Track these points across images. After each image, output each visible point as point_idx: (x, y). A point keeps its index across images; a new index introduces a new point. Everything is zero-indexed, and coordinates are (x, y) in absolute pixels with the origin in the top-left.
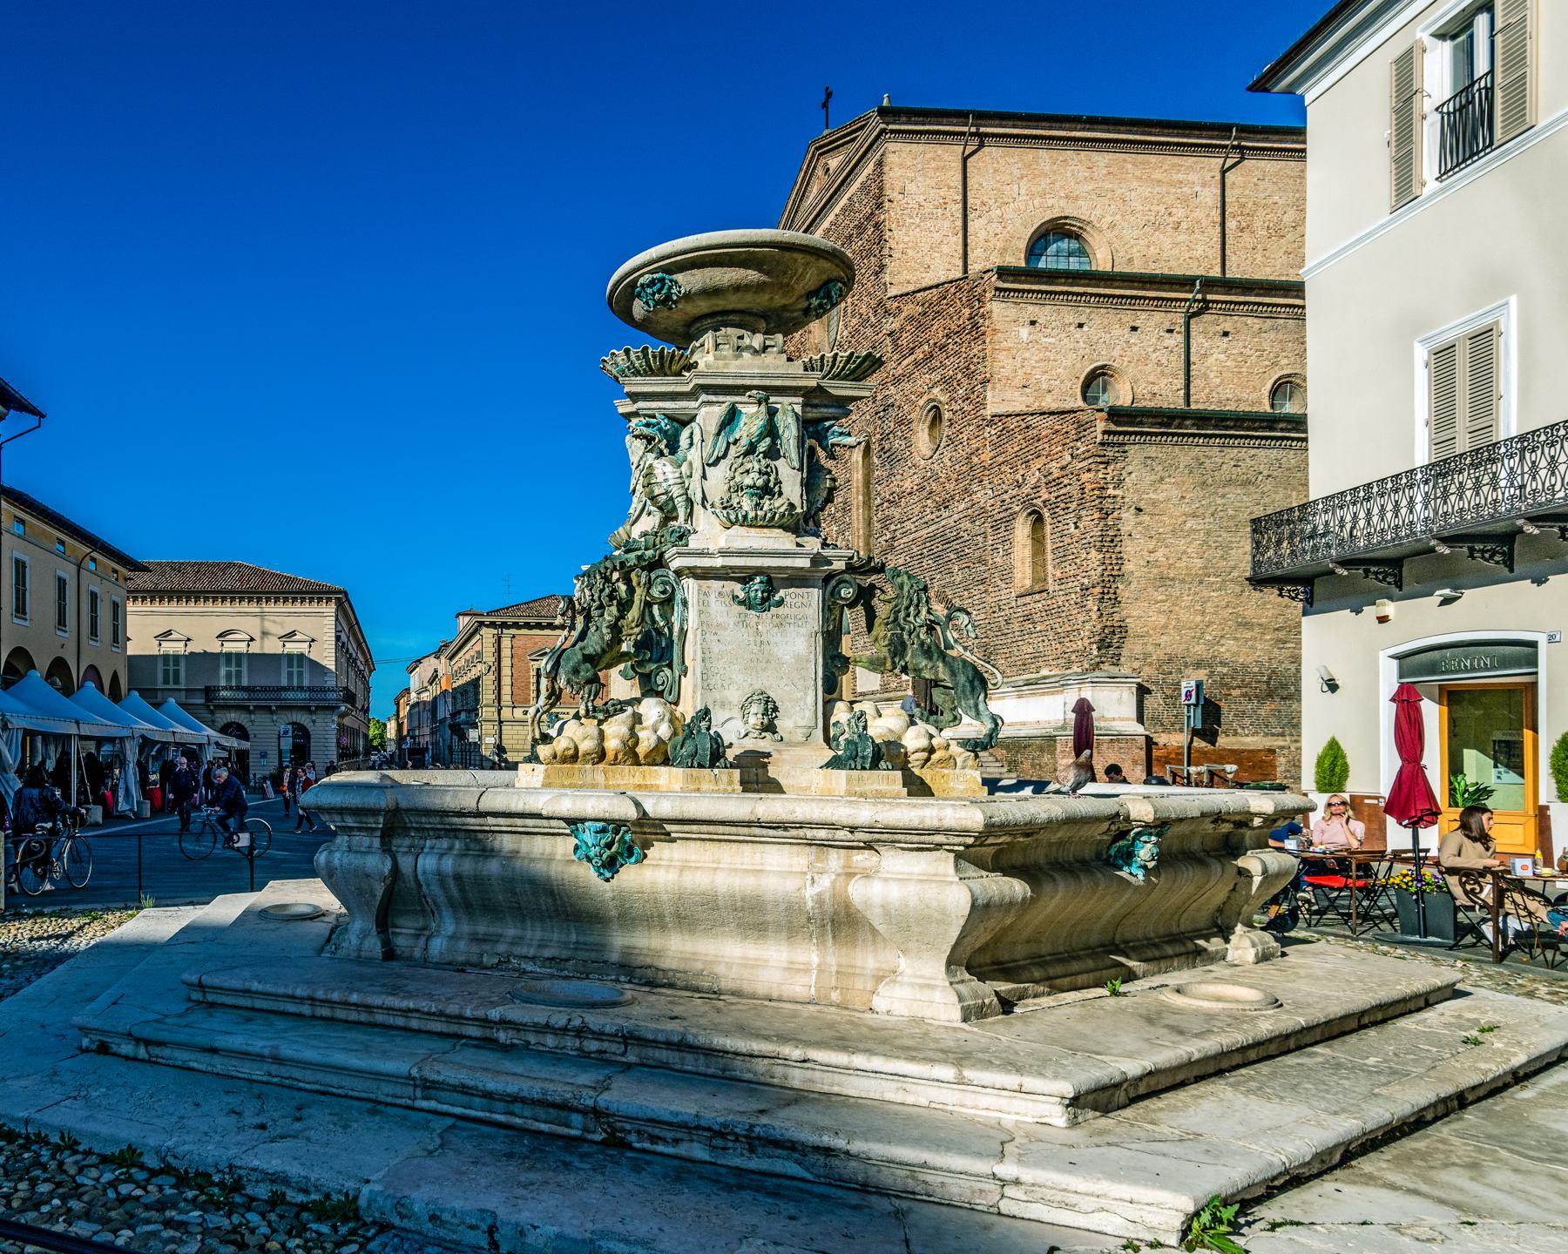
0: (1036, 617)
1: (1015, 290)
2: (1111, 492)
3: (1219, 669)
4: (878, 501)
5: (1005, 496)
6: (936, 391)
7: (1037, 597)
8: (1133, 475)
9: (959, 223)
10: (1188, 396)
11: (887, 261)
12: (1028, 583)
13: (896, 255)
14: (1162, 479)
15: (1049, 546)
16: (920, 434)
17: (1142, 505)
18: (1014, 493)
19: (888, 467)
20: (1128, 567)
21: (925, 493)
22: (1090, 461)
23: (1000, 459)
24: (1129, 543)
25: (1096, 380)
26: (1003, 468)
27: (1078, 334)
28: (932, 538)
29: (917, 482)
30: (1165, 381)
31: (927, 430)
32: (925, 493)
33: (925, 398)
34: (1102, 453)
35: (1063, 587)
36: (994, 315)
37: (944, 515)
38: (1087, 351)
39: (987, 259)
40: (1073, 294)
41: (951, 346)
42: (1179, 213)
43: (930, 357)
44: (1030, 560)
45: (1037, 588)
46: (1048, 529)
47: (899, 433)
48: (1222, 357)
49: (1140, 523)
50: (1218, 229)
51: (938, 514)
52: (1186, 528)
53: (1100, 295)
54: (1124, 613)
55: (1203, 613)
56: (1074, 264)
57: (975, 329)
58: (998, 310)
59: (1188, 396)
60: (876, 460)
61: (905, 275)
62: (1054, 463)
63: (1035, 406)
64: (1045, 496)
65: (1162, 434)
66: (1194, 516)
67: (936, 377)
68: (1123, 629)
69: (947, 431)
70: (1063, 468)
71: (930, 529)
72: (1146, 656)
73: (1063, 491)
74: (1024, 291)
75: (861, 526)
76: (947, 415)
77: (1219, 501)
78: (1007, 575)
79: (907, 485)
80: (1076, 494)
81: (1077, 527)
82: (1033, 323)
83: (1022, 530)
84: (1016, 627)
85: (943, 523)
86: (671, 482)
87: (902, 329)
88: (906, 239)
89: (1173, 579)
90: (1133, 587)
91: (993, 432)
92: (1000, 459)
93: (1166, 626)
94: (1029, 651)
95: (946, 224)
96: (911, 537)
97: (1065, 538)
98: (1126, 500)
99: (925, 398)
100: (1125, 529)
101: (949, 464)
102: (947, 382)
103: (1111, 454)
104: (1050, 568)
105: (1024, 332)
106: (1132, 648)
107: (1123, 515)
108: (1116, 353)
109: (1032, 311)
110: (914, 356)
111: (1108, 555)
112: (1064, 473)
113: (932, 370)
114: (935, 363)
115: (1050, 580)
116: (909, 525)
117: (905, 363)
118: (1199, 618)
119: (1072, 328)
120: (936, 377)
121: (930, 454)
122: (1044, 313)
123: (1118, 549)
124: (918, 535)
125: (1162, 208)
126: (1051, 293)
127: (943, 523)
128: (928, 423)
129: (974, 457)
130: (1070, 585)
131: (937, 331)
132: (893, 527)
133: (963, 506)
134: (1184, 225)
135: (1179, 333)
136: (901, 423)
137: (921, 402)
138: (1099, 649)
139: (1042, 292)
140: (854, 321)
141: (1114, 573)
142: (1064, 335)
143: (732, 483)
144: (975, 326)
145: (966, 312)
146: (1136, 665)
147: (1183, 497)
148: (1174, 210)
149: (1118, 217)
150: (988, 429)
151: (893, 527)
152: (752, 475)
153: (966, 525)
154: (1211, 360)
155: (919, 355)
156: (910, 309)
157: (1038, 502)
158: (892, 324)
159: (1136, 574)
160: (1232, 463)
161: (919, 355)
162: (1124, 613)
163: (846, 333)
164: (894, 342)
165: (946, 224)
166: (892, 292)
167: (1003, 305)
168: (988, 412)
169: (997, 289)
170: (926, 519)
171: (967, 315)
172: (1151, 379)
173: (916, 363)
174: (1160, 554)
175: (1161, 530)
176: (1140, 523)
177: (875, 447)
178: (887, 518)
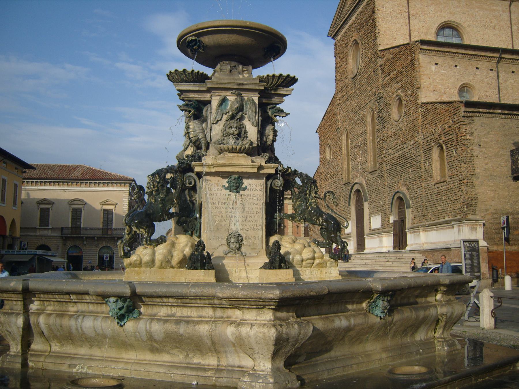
0: (443, 194)
1: (428, 50)
2: (468, 137)
3: (516, 216)
4: (378, 140)
5: (428, 139)
6: (399, 91)
7: (442, 184)
8: (477, 130)
9: (407, 21)
10: (499, 97)
11: (377, 35)
12: (439, 178)
14: (488, 133)
15: (446, 161)
16: (393, 110)
17: (481, 144)
18: (432, 137)
19: (382, 125)
20: (477, 171)
21: (397, 137)
22: (459, 124)
23: (425, 122)
24: (477, 160)
25: (463, 89)
26: (427, 126)
27: (455, 69)
28: (400, 157)
29: (393, 131)
30: (491, 91)
31: (397, 109)
32: (397, 137)
33: (395, 94)
34: (464, 120)
35: (452, 179)
36: (421, 60)
37: (405, 147)
38: (459, 77)
39: (420, 36)
40: (452, 53)
41: (404, 72)
42: (495, 22)
43: (396, 76)
44: (439, 167)
45: (442, 180)
46: (445, 154)
47: (385, 109)
48: (512, 81)
49: (481, 151)
50: (510, 30)
51: (402, 146)
52: (500, 154)
53: (463, 54)
54: (477, 191)
55: (509, 191)
56: (456, 41)
57: (413, 64)
58: (423, 59)
59: (499, 97)
60: (377, 121)
62: (446, 125)
63: (439, 100)
64: (444, 139)
65: (488, 113)
66: (503, 148)
67: (399, 85)
68: (476, 198)
70: (450, 127)
71: (400, 153)
72: (487, 210)
73: (450, 137)
74: (432, 50)
75: (372, 151)
76: (404, 102)
78: (431, 176)
80: (455, 138)
81: (456, 153)
82: (437, 64)
83: (435, 153)
84: (435, 197)
85: (404, 150)
86: (197, 131)
87: (385, 64)
88: (386, 26)
89: (495, 176)
90: (480, 178)
91: (422, 110)
92: (425, 122)
93: (494, 197)
94: (441, 209)
95: (402, 21)
96: (392, 156)
97: (452, 158)
98: (475, 141)
99: (395, 94)
100: (475, 154)
101: (406, 124)
102: (402, 87)
103: (468, 121)
104: (447, 171)
105: (434, 68)
106: (480, 207)
107: (475, 148)
108: (471, 78)
109: (436, 59)
110: (390, 76)
111: (469, 165)
112: (450, 129)
113: (398, 82)
114: (398, 79)
115: (447, 177)
116: (391, 151)
117: (387, 79)
118: (507, 193)
119: (452, 67)
120: (399, 85)
122: (440, 60)
123: (473, 163)
124: (394, 155)
125: (488, 20)
126: (443, 52)
127: (404, 150)
128: (397, 105)
129: (415, 121)
130: (455, 179)
131: (399, 66)
132: (384, 152)
134: (497, 27)
135: (495, 71)
136: (386, 105)
137: (394, 96)
138: (467, 208)
139: (440, 51)
140: (366, 60)
141: (472, 173)
142: (450, 70)
143: (224, 132)
144: (413, 64)
145: (409, 58)
146: (483, 215)
147: (497, 140)
148: (493, 21)
149: (471, 22)
150: (420, 109)
151: (384, 152)
152: (233, 129)
153: (413, 151)
154: (508, 82)
155: (392, 75)
156: (388, 56)
157: (441, 141)
158: (380, 62)
159: (481, 174)
160: (516, 126)
161: (392, 75)
162: (477, 191)
163: (363, 65)
164: (383, 71)
165: (402, 21)
166: (381, 48)
167: (424, 56)
168: (419, 102)
169: (421, 49)
170: (397, 149)
171: (410, 59)
172: (486, 89)
173: (391, 79)
174: (490, 165)
175: (490, 154)
176: (481, 151)
178: (382, 148)
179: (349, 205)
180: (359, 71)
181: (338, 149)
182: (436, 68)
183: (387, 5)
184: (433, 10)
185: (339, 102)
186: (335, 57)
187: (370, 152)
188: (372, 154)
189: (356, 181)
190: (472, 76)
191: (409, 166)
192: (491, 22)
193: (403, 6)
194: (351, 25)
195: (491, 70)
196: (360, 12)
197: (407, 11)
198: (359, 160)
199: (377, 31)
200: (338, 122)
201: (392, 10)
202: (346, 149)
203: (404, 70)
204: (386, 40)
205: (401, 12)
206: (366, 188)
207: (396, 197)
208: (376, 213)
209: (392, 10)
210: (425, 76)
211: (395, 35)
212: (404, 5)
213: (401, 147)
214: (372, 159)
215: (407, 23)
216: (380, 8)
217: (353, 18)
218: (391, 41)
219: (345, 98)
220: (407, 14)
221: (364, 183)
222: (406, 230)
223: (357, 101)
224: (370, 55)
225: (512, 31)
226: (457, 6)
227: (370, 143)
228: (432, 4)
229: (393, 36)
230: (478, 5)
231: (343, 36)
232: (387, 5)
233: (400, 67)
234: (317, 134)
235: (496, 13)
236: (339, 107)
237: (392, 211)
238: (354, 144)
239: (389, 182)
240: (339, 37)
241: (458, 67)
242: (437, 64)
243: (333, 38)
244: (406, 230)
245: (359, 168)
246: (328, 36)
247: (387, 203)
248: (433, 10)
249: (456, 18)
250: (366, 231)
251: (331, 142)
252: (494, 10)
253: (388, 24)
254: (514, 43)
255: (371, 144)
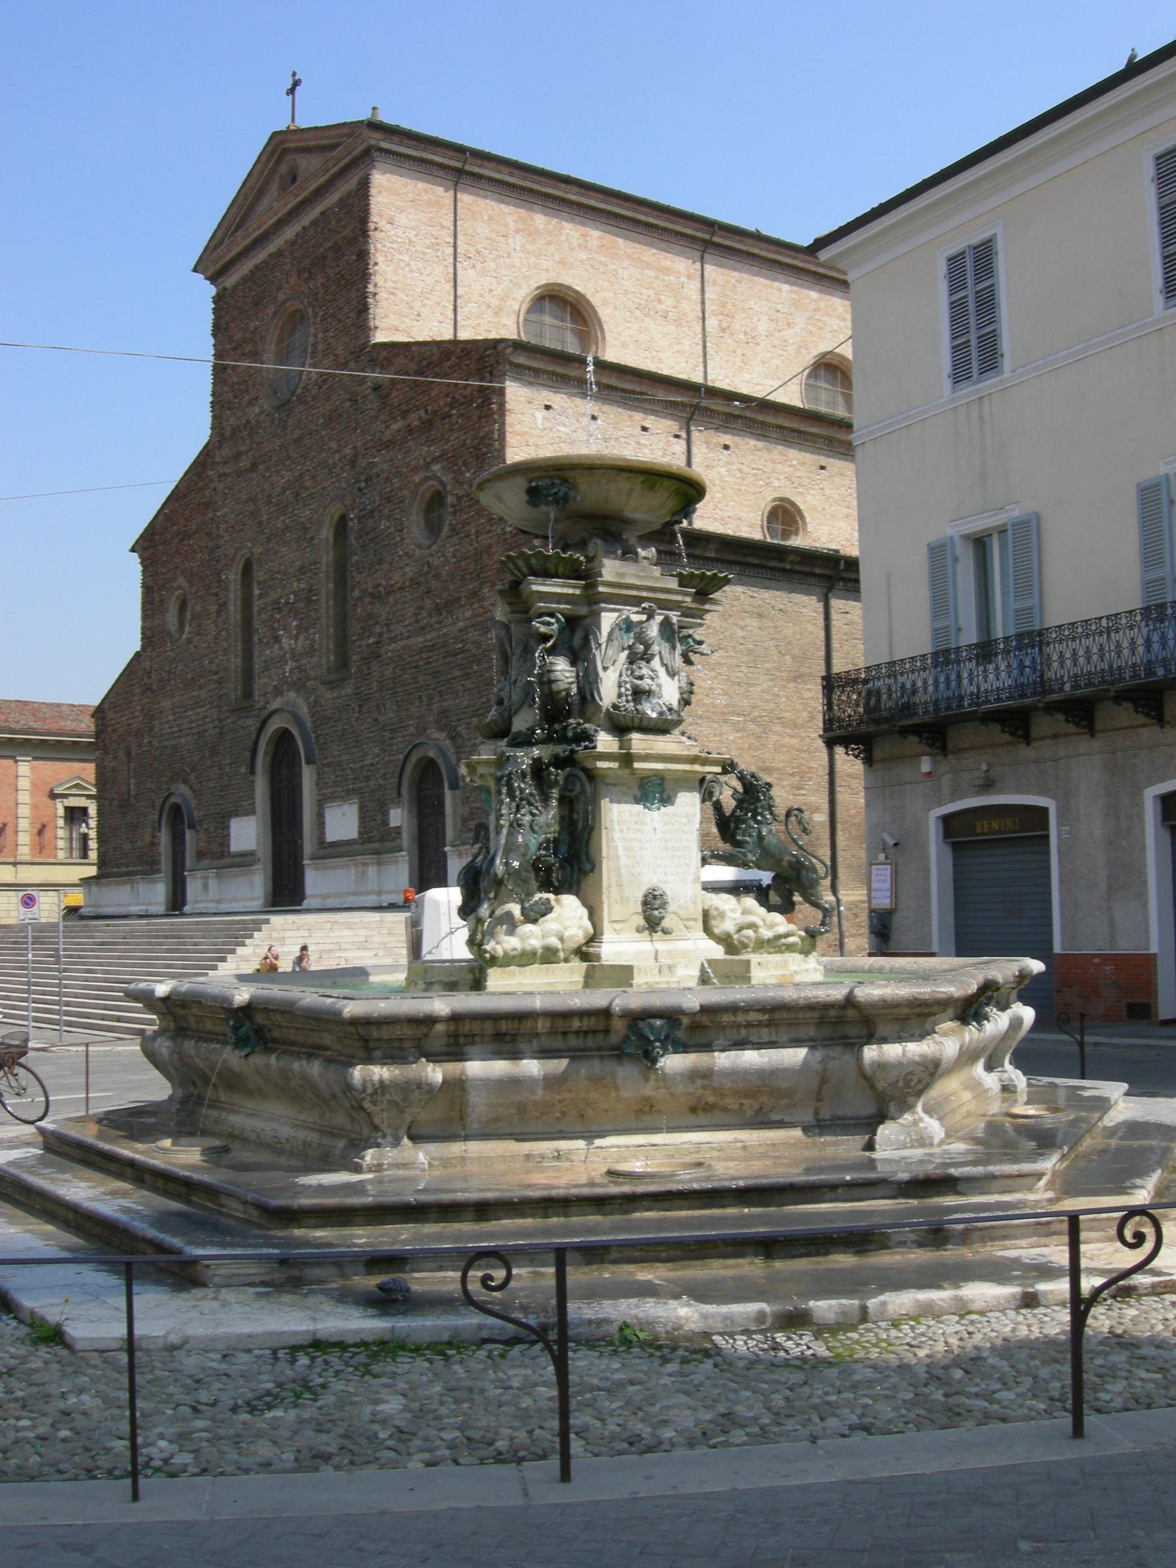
1: (529, 368)
6: (436, 467)
13: (382, 295)
28: (432, 648)
43: (428, 424)
61: (393, 320)
67: (435, 450)
69: (449, 520)
76: (450, 500)
77: (740, 633)
79: (396, 577)
82: (548, 407)
95: (439, 269)
105: (540, 415)
116: (397, 629)
120: (435, 450)
121: (428, 543)
132: (378, 629)
133: (468, 614)
165: (439, 269)
173: (410, 430)
177: (353, 524)
178: (370, 616)
179: (252, 771)
180: (299, 391)
181: (214, 608)
182: (545, 419)
183: (402, 219)
184: (518, 248)
185: (221, 469)
186: (214, 335)
187: (328, 627)
188: (332, 630)
189: (274, 705)
190: (630, 447)
191: (457, 673)
192: (659, 301)
193: (443, 227)
194: (279, 253)
195: (677, 436)
196: (314, 223)
197: (452, 240)
198: (286, 646)
199: (371, 288)
200: (218, 528)
201: (414, 233)
202: (239, 609)
203: (454, 412)
204: (392, 316)
205: (438, 244)
206: (309, 725)
207: (414, 758)
208: (345, 797)
209: (414, 233)
210: (518, 437)
211: (417, 305)
212: (445, 223)
213: (434, 620)
214: (331, 646)
215: (452, 276)
216: (382, 224)
217: (290, 233)
218: (407, 320)
219: (244, 463)
220: (451, 250)
221: (304, 711)
222: (446, 849)
223: (288, 475)
224: (340, 350)
225: (704, 329)
226: (580, 245)
227: (327, 601)
228: (518, 231)
229: (411, 308)
230: (629, 251)
231: (245, 280)
232: (402, 219)
233: (442, 403)
234: (136, 555)
235: (672, 278)
236: (220, 486)
237: (399, 795)
238: (273, 596)
239: (391, 715)
240: (231, 281)
241: (599, 421)
242: (548, 407)
243: (213, 279)
244: (446, 849)
245: (287, 668)
246: (195, 270)
247: (382, 772)
248: (518, 248)
249: (578, 281)
250: (308, 845)
251: (185, 585)
252: (668, 269)
253: (400, 272)
254: (709, 362)
255: (331, 603)
